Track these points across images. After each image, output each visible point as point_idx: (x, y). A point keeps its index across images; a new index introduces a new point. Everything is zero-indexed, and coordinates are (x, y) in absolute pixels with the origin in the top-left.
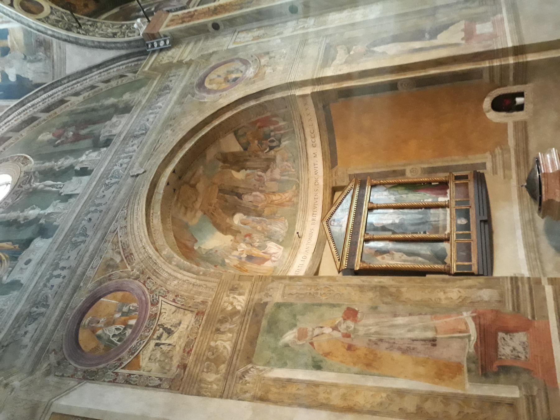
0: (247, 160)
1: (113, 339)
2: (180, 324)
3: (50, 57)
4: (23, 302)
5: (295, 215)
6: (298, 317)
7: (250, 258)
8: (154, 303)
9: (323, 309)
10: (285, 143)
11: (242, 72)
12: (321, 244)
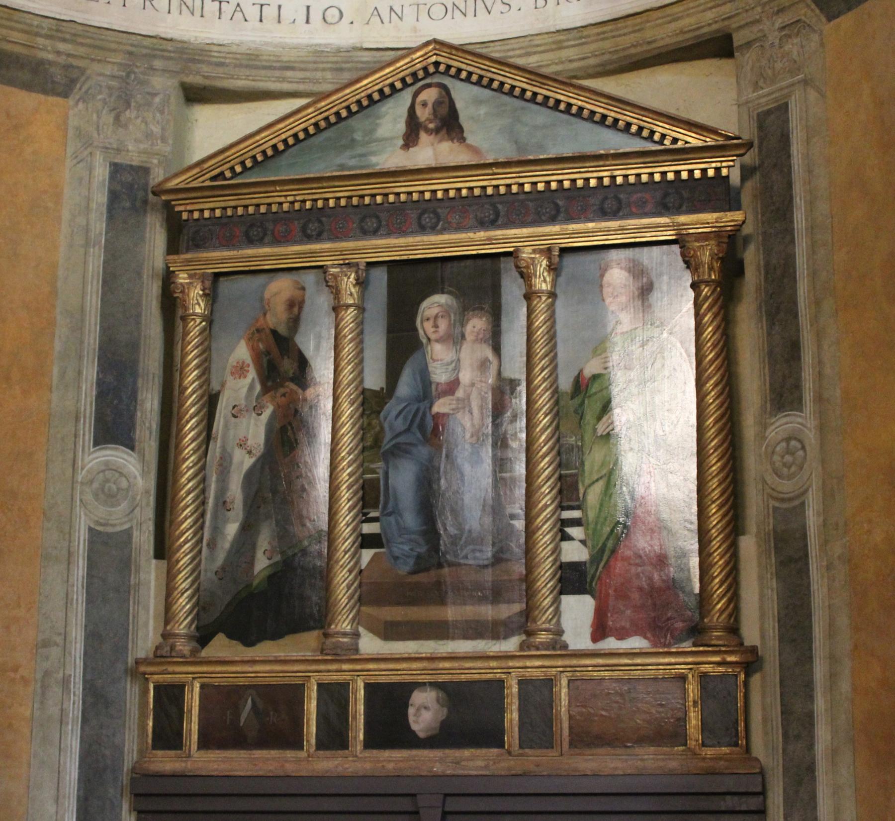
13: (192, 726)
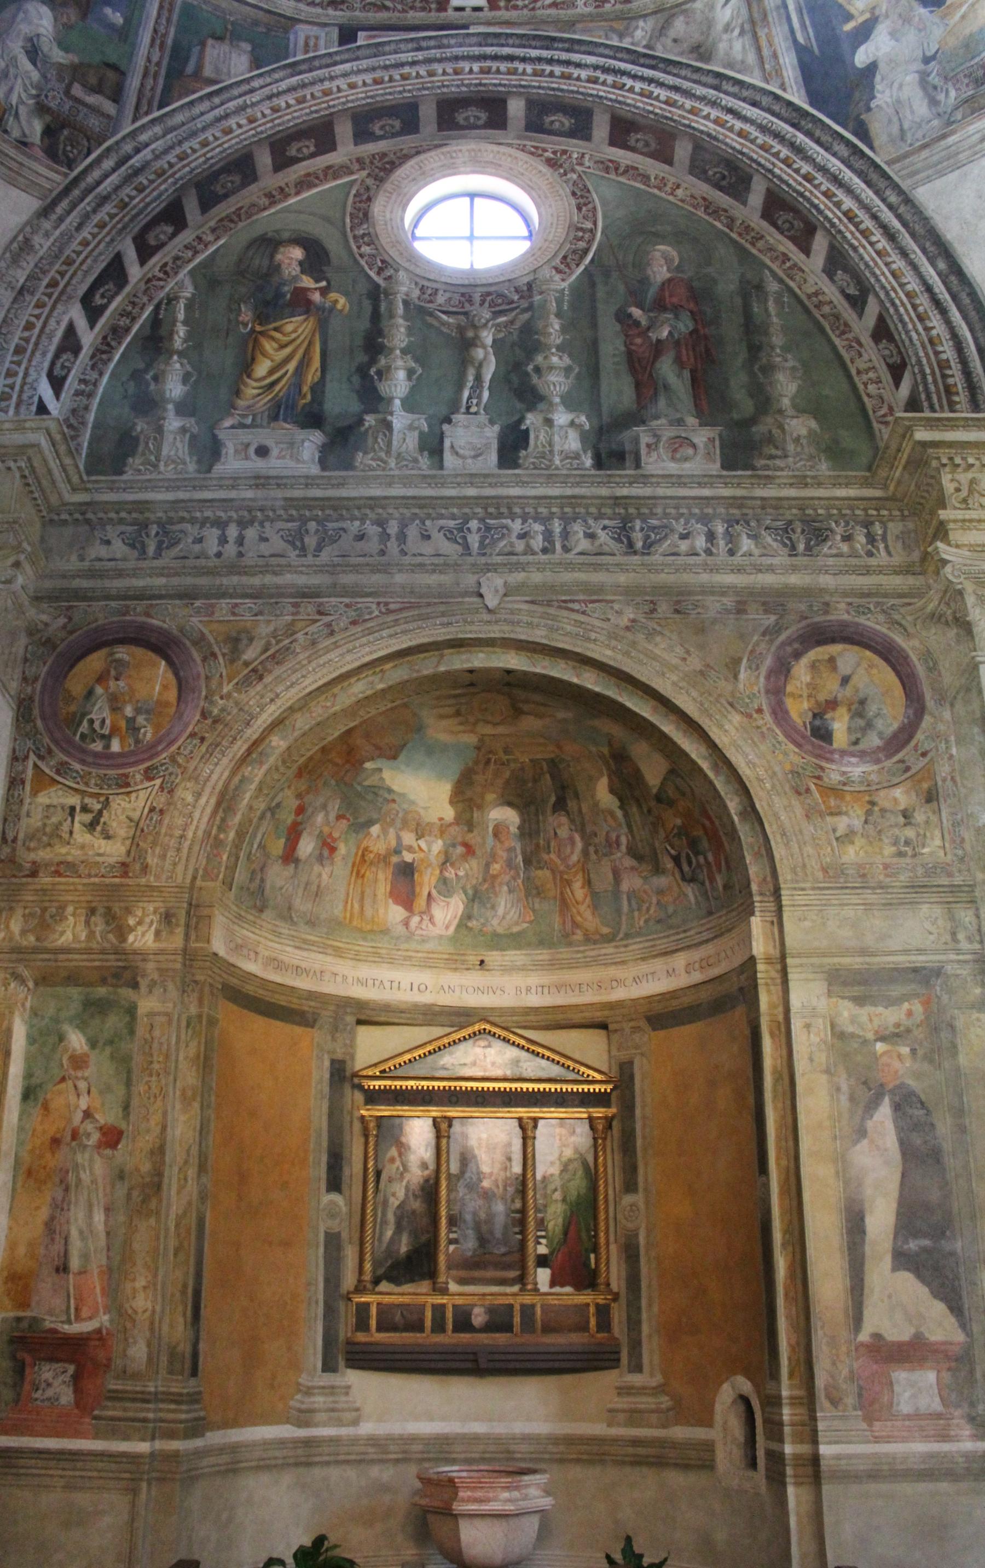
0: (640, 806)
1: (85, 723)
2: (108, 837)
3: (949, 123)
4: (170, 496)
5: (541, 943)
6: (108, 1050)
7: (407, 872)
8: (149, 775)
9: (121, 1090)
10: (690, 891)
11: (856, 742)
12: (462, 1019)
13: (373, 1323)
